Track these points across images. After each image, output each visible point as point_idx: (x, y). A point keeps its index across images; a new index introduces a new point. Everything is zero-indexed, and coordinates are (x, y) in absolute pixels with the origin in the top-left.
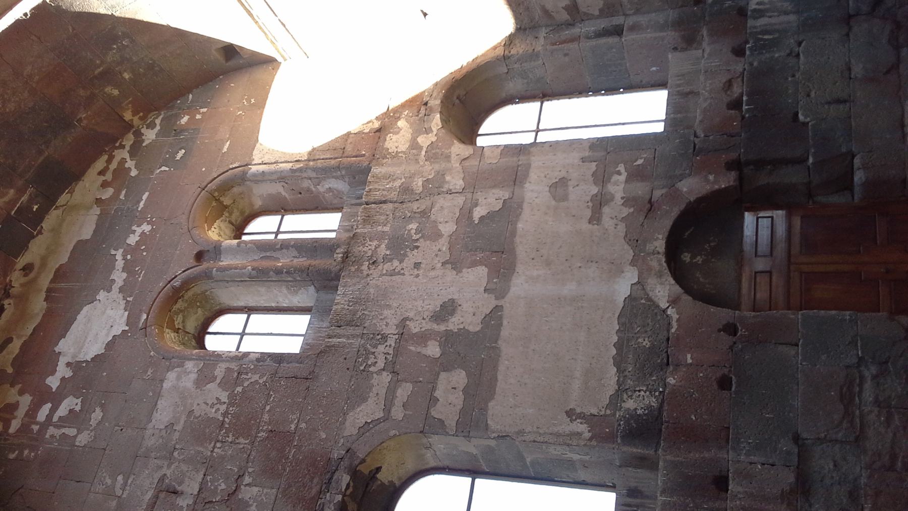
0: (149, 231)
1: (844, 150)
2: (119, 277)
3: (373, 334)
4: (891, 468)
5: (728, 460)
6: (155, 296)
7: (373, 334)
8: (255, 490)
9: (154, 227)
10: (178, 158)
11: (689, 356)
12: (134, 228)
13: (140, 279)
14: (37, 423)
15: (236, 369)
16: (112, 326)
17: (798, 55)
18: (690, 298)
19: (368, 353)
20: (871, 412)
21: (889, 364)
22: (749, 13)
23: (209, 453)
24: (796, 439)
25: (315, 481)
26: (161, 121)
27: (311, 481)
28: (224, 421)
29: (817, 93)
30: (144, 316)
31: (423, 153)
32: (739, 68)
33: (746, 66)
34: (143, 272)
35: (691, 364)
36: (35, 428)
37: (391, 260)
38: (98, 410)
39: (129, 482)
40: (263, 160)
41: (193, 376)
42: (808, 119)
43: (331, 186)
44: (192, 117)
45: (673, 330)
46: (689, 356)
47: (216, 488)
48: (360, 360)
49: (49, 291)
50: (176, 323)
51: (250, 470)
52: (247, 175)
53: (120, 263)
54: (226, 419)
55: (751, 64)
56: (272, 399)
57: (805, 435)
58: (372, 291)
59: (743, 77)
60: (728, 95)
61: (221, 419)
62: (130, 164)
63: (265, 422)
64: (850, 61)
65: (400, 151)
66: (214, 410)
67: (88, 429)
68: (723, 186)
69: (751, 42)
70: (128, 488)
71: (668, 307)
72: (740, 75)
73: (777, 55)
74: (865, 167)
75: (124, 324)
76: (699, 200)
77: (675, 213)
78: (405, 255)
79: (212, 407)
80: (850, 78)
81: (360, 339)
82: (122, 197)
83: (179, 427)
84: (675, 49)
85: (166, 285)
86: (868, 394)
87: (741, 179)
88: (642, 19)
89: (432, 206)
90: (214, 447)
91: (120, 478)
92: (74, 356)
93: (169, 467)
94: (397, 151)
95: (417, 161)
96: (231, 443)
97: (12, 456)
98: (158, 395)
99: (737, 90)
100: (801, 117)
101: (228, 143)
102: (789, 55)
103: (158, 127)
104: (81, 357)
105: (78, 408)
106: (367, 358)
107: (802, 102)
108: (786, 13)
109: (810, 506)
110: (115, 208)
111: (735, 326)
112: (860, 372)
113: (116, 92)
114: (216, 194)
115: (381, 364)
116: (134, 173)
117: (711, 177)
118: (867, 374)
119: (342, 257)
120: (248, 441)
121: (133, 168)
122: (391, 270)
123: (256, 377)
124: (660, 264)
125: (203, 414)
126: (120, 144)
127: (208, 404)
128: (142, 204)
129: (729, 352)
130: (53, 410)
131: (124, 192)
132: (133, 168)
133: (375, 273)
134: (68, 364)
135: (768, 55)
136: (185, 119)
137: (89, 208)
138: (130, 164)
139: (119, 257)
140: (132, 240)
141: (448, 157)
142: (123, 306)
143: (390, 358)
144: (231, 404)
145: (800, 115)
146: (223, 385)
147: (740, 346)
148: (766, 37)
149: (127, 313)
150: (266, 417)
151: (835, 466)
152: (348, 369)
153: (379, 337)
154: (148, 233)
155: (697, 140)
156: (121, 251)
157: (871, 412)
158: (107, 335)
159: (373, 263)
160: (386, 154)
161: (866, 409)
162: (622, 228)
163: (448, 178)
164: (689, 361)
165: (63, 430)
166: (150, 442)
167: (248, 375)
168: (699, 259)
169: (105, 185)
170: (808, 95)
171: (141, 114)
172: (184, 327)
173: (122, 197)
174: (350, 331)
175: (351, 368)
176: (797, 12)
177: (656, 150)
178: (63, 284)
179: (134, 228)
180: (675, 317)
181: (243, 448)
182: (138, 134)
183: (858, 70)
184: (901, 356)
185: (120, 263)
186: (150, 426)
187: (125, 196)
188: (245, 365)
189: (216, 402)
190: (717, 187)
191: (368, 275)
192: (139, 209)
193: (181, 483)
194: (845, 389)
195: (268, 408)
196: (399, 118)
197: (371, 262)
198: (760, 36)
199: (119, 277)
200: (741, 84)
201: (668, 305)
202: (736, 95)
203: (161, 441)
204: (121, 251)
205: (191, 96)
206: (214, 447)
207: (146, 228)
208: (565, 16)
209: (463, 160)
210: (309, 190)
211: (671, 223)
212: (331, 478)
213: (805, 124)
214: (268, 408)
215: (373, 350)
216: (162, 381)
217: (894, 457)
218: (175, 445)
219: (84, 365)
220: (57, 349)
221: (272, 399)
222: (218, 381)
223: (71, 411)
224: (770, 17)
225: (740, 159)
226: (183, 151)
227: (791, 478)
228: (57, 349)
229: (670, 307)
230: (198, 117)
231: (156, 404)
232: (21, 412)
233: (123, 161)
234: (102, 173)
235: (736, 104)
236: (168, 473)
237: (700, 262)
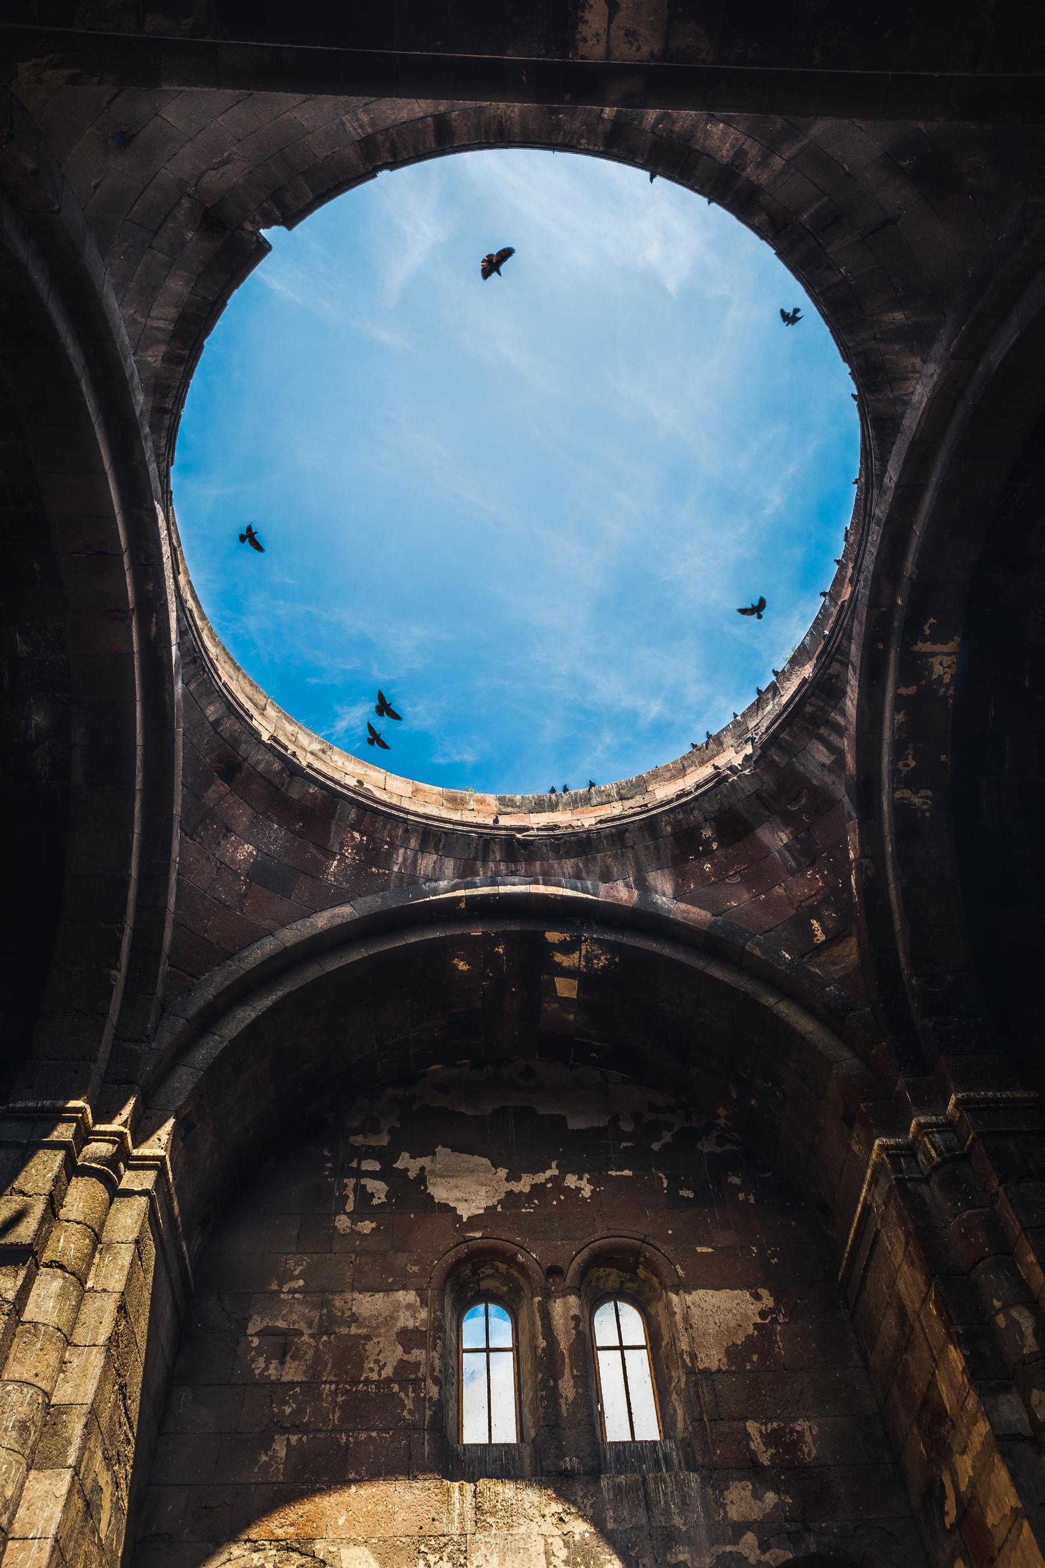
0: (583, 1196)
2: (524, 1185)
3: (466, 1551)
7: (466, 1551)
8: (282, 1453)
9: (589, 1200)
10: (682, 1193)
12: (586, 1176)
13: (523, 1210)
14: (359, 1164)
15: (419, 1375)
16: (466, 1201)
23: (324, 1379)
25: (291, 1530)
27: (292, 1525)
28: (360, 1382)
30: (478, 1235)
31: (729, 1548)
34: (532, 1211)
36: (354, 1164)
37: (566, 1544)
39: (297, 1296)
40: (692, 1307)
41: (411, 1324)
44: (738, 1189)
47: (287, 1403)
48: (433, 1542)
50: (483, 1270)
51: (305, 1439)
53: (541, 1178)
54: (361, 1385)
56: (384, 1435)
58: (522, 1529)
61: (362, 1379)
62: (667, 1137)
63: (357, 1437)
65: (728, 1509)
66: (372, 1365)
67: (352, 1224)
70: (290, 1296)
75: (470, 1214)
79: (377, 1361)
81: (458, 1532)
82: (624, 1144)
83: (354, 1330)
85: (517, 1245)
90: (331, 1383)
91: (301, 1283)
93: (311, 1336)
94: (726, 1504)
95: (714, 1541)
96: (336, 1402)
97: (326, 1153)
98: (388, 1289)
101: (710, 1250)
103: (719, 1150)
104: (431, 1180)
105: (375, 1202)
106: (434, 1551)
113: (734, 1095)
116: (655, 1146)
119: (566, 1469)
120: (336, 1422)
121: (662, 1142)
122: (552, 1550)
123: (409, 1404)
125: (368, 1353)
127: (378, 1355)
128: (613, 1173)
130: (373, 1175)
131: (630, 1144)
132: (662, 1142)
133: (548, 1526)
134: (422, 1169)
136: (735, 1180)
138: (667, 1137)
139: (549, 1173)
140: (571, 1181)
142: (490, 1204)
144: (378, 1383)
146: (402, 1366)
149: (482, 1211)
150: (363, 1436)
152: (421, 1528)
153: (463, 1561)
154: (580, 1196)
156: (556, 1172)
159: (561, 1519)
160: (722, 1487)
165: (351, 1196)
166: (338, 1302)
167: (412, 1393)
172: (483, 1278)
173: (624, 1144)
174: (470, 1514)
175: (422, 1533)
178: (513, 1123)
179: (586, 1176)
181: (330, 1420)
185: (541, 1178)
186: (356, 1295)
187: (625, 1148)
188: (425, 1385)
189: (381, 1364)
191: (544, 1516)
192: (610, 1173)
193: (294, 1358)
195: (374, 1434)
196: (777, 1491)
197: (562, 1515)
199: (524, 1185)
203: (339, 1314)
204: (556, 1172)
206: (331, 1383)
212: (294, 1550)
214: (374, 1434)
215: (445, 1558)
216: (405, 1288)
218: (335, 1333)
219: (422, 1188)
220: (439, 1149)
221: (384, 1435)
222: (406, 1357)
223: (372, 1195)
226: (692, 1195)
228: (439, 1149)
230: (741, 1196)
231: (379, 1291)
232: (373, 1141)
236: (305, 1338)
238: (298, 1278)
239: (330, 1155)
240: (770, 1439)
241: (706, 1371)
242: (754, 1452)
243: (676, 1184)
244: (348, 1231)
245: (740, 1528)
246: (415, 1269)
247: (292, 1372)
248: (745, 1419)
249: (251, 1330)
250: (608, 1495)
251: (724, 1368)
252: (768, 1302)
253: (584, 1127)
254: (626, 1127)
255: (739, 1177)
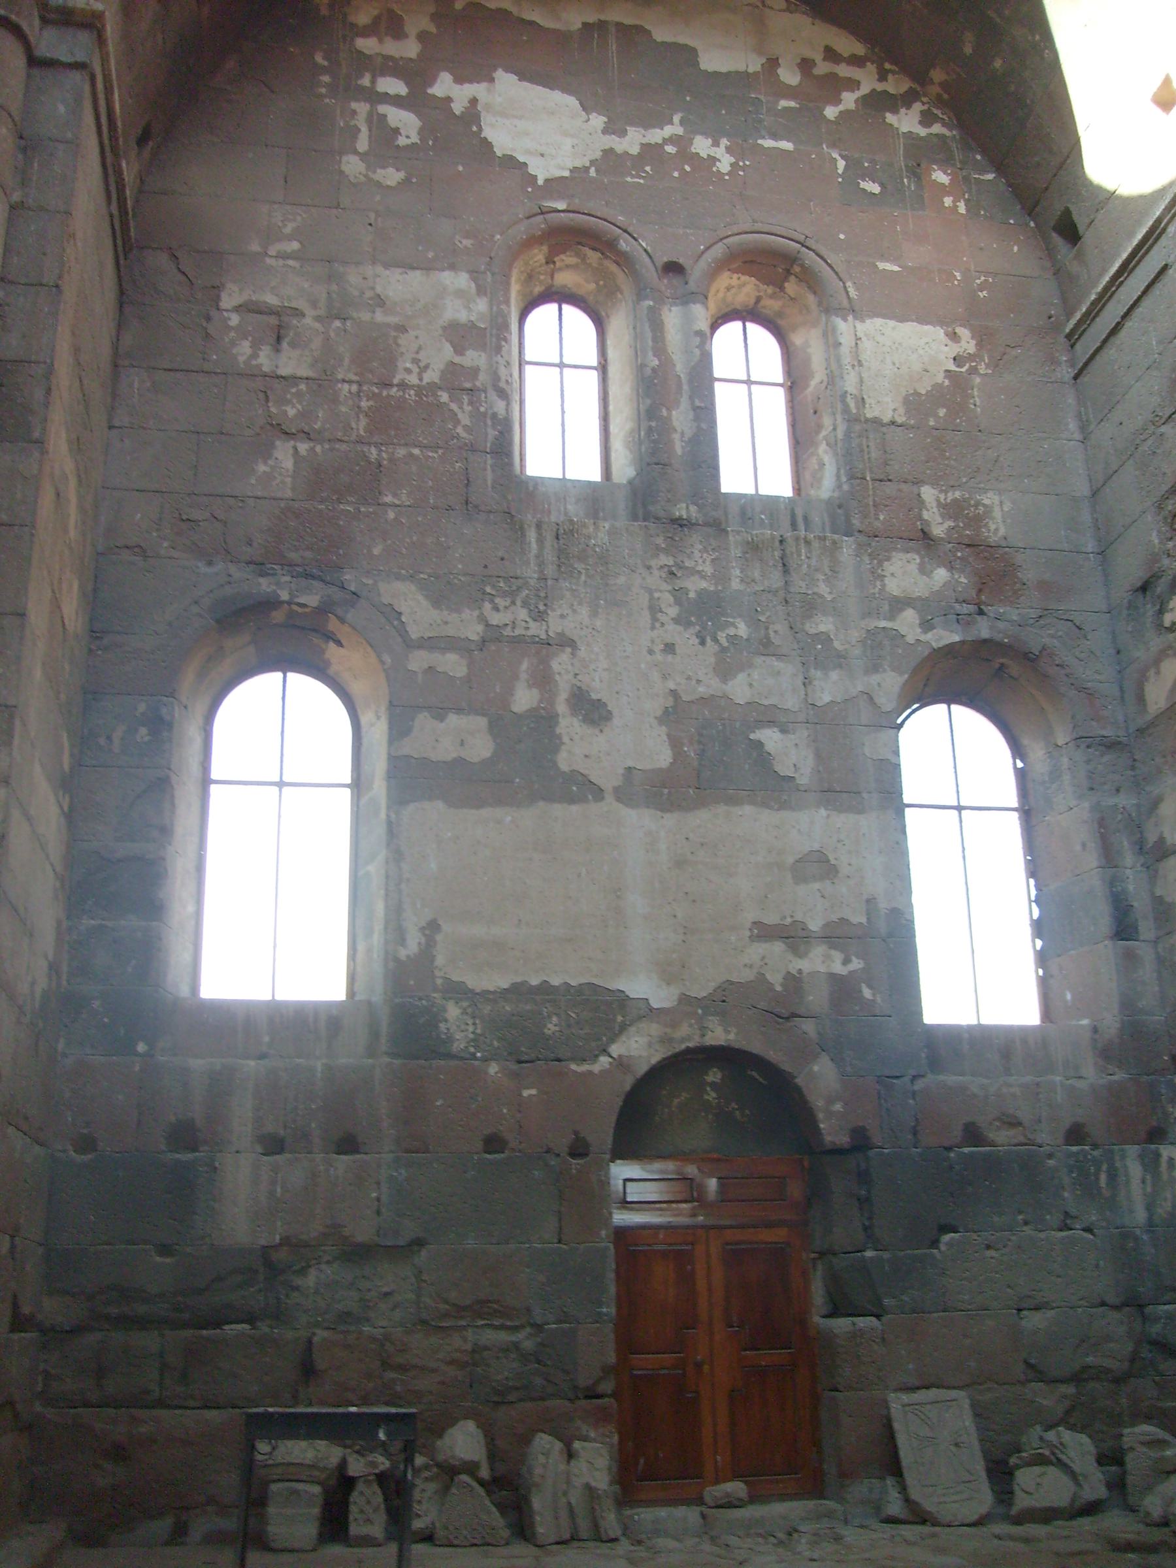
0: (719, 171)
1: (886, 1301)
2: (632, 141)
3: (546, 597)
4: (386, 1365)
5: (380, 1153)
6: (599, 214)
7: (546, 597)
8: (289, 464)
9: (727, 177)
10: (863, 185)
11: (533, 1092)
12: (724, 142)
13: (629, 179)
14: (373, 82)
15: (478, 384)
16: (542, 155)
17: (1065, 1227)
18: (628, 1087)
19: (512, 594)
20: (465, 1340)
21: (536, 1365)
22: (1153, 1146)
23: (340, 377)
24: (419, 1243)
25: (308, 554)
26: (937, 135)
27: (308, 548)
28: (391, 385)
29: (993, 1261)
30: (561, 206)
31: (883, 624)
32: (1043, 1137)
33: (1048, 1148)
34: (642, 181)
35: (520, 1095)
36: (366, 81)
37: (678, 602)
38: (401, 175)
39: (291, 262)
40: (864, 339)
41: (463, 316)
42: (943, 1248)
43: (827, 467)
44: (943, 190)
45: (573, 1067)
46: (533, 1092)
47: (289, 402)
48: (502, 584)
49: (602, 25)
50: (563, 257)
51: (318, 449)
52: (834, 317)
53: (656, 136)
54: (395, 389)
55: (1050, 1156)
56: (430, 454)
57: (424, 1253)
58: (622, 580)
59: (1026, 1144)
60: (991, 1124)
61: (396, 381)
62: (849, 100)
63: (393, 453)
64: (1052, 1309)
65: (886, 582)
66: (408, 365)
67: (368, 169)
68: (822, 1126)
69: (1095, 1153)
70: (281, 262)
71: (611, 1057)
72: (1029, 1139)
73: (1066, 1194)
74: (856, 1335)
75: (549, 176)
76: (798, 1090)
77: (772, 1055)
78: (688, 624)
79: (416, 361)
80: (1019, 1310)
81: (536, 576)
82: (783, 103)
83: (380, 317)
84: (1095, 1030)
85: (619, 228)
86: (490, 1337)
87: (838, 1152)
88: (1147, 971)
89: (780, 656)
90: (350, 382)
91: (295, 245)
92: (488, 107)
93: (318, 318)
94: (885, 576)
95: (866, 615)
96: (359, 407)
97: (319, 59)
98: (428, 267)
99: (1002, 1137)
100: (946, 1238)
101: (896, 268)
102: (1066, 1214)
103: (923, 132)
104: (486, 119)
105: (402, 141)
106: (504, 594)
107: (976, 1238)
108: (1150, 1207)
109: (328, 1262)
110: (762, 97)
111: (586, 1155)
112: (523, 1327)
114: (797, 269)
115: (496, 619)
116: (831, 112)
117: (838, 1107)
118: (520, 1336)
119: (680, 518)
120: (362, 433)
121: (841, 108)
122: (659, 606)
123: (465, 419)
124: (683, 1040)
125: (403, 350)
126: (888, 71)
127: (417, 353)
128: (768, 143)
129: (542, 1148)
130: (397, 101)
131: (792, 104)
132: (841, 108)
133: (655, 579)
134: (474, 101)
135: (1066, 1181)
136: (941, 177)
137: (759, 50)
138: (849, 100)
139: (668, 131)
140: (702, 146)
141: (875, 668)
142: (578, 164)
143: (507, 632)
144: (419, 390)
145: (953, 1234)
146: (452, 370)
147: (553, 1163)
148: (1103, 1178)
149: (566, 174)
150: (401, 452)
151: (386, 1294)
152: (486, 567)
153: (542, 608)
154: (714, 169)
155: (907, 1079)
156: (680, 131)
157: (465, 1340)
158: (528, 152)
159: (672, 573)
160: (880, 558)
161: (469, 1334)
162: (747, 976)
163: (834, 675)
164: (526, 1093)
165: (364, 129)
166: (353, 278)
167: (468, 405)
168: (711, 1096)
169: (806, 65)
170: (988, 1247)
171: (946, 96)
172: (560, 269)
173: (783, 103)
174: (550, 556)
176: (1151, 1224)
177: (890, 1016)
178: (614, 47)
179: (724, 142)
180: (596, 1068)
181: (352, 429)
182: (908, 99)
183: (1034, 1321)
184: (546, 1379)
185: (656, 136)
186: (379, 269)
187: (785, 109)
188: (486, 397)
189: (422, 364)
190: (821, 1116)
191: (649, 568)
192: (760, 141)
193: (293, 345)
194: (495, 1306)
195: (416, 451)
196: (951, 568)
197: (673, 569)
198: (1105, 1167)
199: (632, 141)
200: (1015, 1141)
201: (615, 1055)
202: (991, 1135)
204: (680, 131)
205: (990, 176)
206: (350, 382)
207: (725, 164)
208: (1151, 838)
209: (870, 696)
210: (820, 427)
211: (754, 1051)
212: (313, 577)
213: (935, 1243)
214: (416, 451)
215: (519, 603)
216: (452, 267)
217: (403, 1368)
218: (352, 319)
219: (475, 129)
220: (500, 74)
221: (430, 454)
222: (457, 360)
223: (396, 131)
224: (1143, 1181)
225: (871, 1149)
227: (360, 1238)
228: (500, 74)
229: (610, 1060)
230: (948, 201)
231: (413, 268)
232: (391, 48)
233: (853, 84)
234: (831, 54)
235: (973, 1135)
236: (308, 321)
237: (706, 1097)
238: (290, 238)
239: (326, 63)
240: (952, 510)
241: (876, 421)
242: (927, 523)
243: (855, 169)
244: (362, 179)
245: (898, 604)
246: (467, 243)
247: (291, 363)
248: (918, 482)
249: (227, 302)
250: (735, 552)
251: (900, 420)
252: (968, 344)
253: (724, 70)
254: (789, 76)
255: (948, 175)
